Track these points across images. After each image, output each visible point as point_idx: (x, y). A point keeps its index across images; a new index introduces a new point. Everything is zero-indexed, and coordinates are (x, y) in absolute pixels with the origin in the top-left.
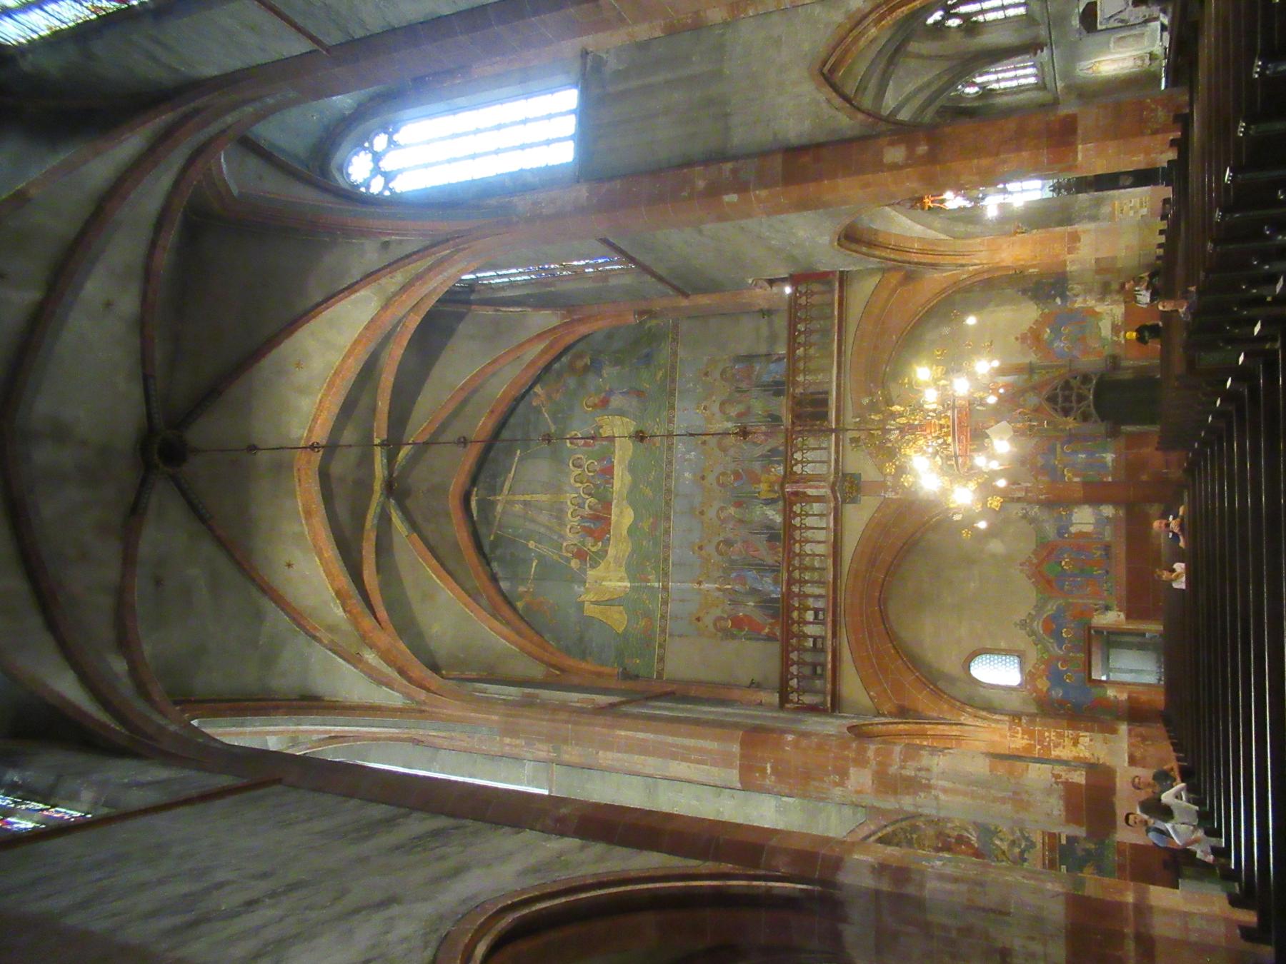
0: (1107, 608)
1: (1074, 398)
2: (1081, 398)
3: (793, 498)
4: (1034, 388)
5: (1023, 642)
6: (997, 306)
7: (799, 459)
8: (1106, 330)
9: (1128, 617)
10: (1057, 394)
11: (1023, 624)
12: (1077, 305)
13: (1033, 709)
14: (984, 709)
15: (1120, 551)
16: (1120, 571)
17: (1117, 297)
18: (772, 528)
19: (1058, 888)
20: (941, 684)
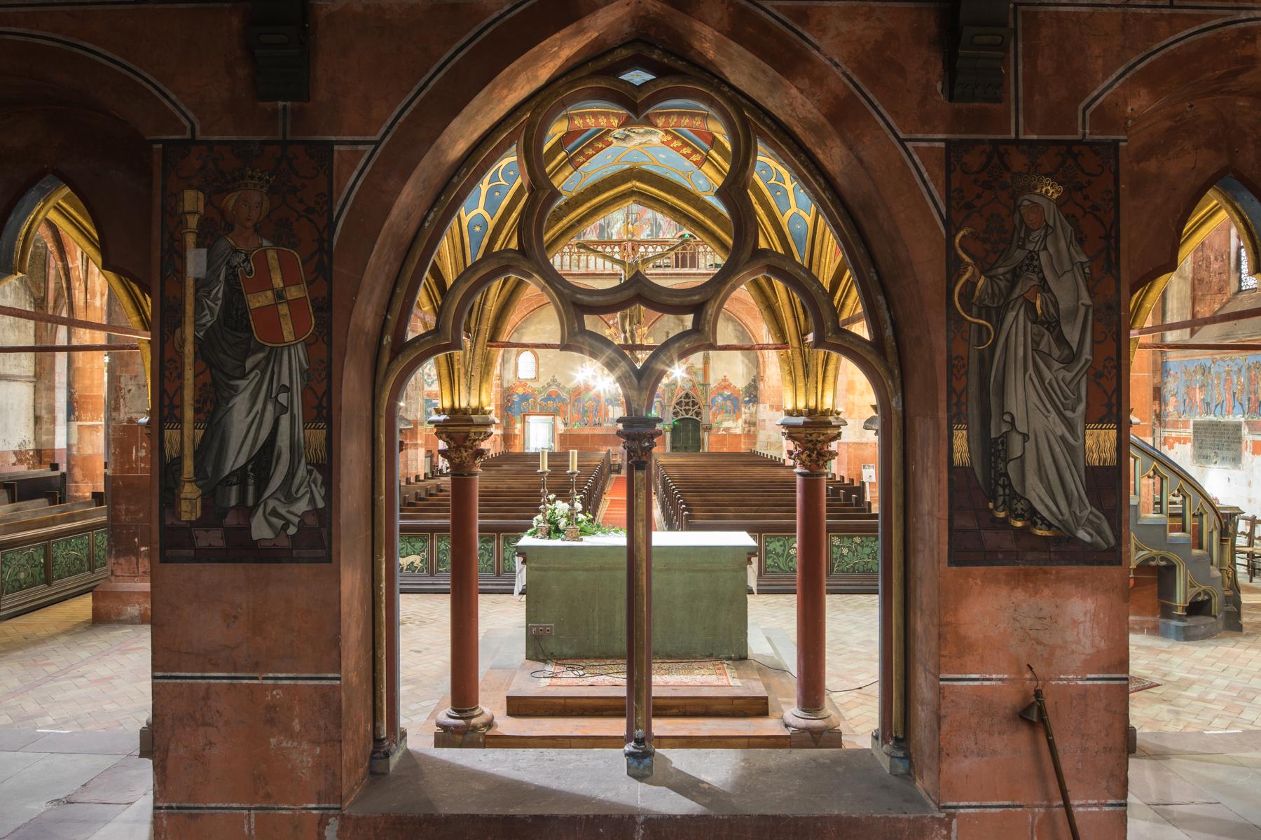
0: (566, 424)
1: (687, 407)
2: (687, 411)
3: (622, 247)
4: (694, 386)
5: (544, 380)
6: (747, 365)
7: (649, 250)
8: (726, 424)
9: (561, 435)
10: (689, 398)
11: (554, 381)
12: (743, 409)
13: (505, 385)
14: (503, 360)
15: (598, 431)
16: (587, 431)
17: (746, 429)
18: (608, 227)
19: (419, 417)
20: (515, 334)
